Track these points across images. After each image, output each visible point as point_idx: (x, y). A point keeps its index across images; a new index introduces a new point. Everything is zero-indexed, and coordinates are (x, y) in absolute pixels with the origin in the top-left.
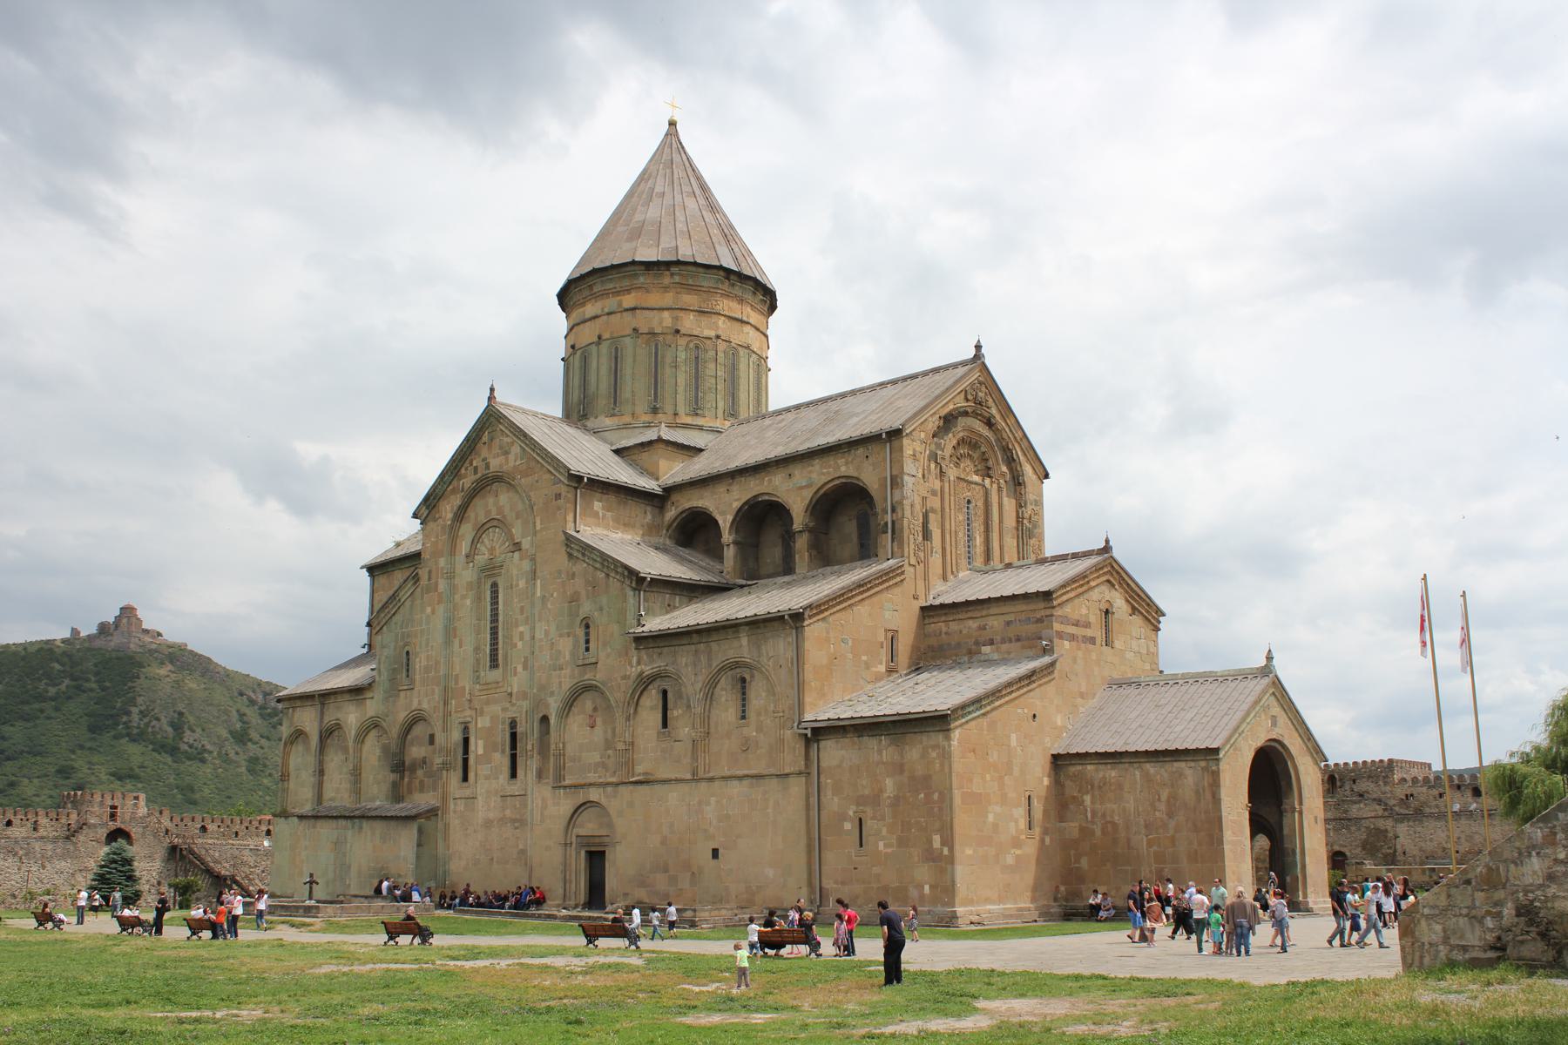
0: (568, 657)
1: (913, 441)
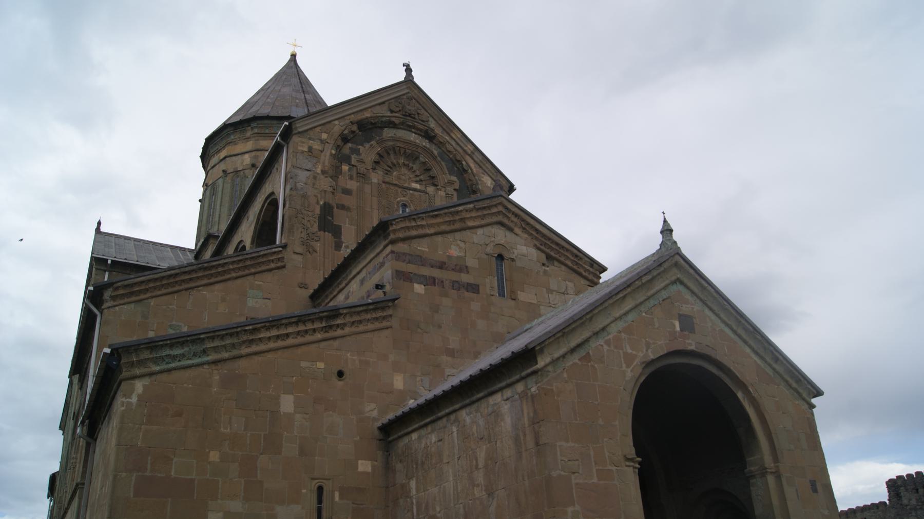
1: (310, 139)
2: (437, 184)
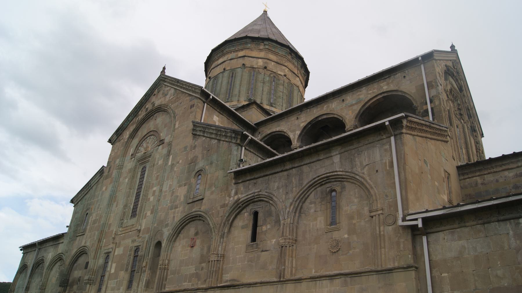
0: (182, 199)
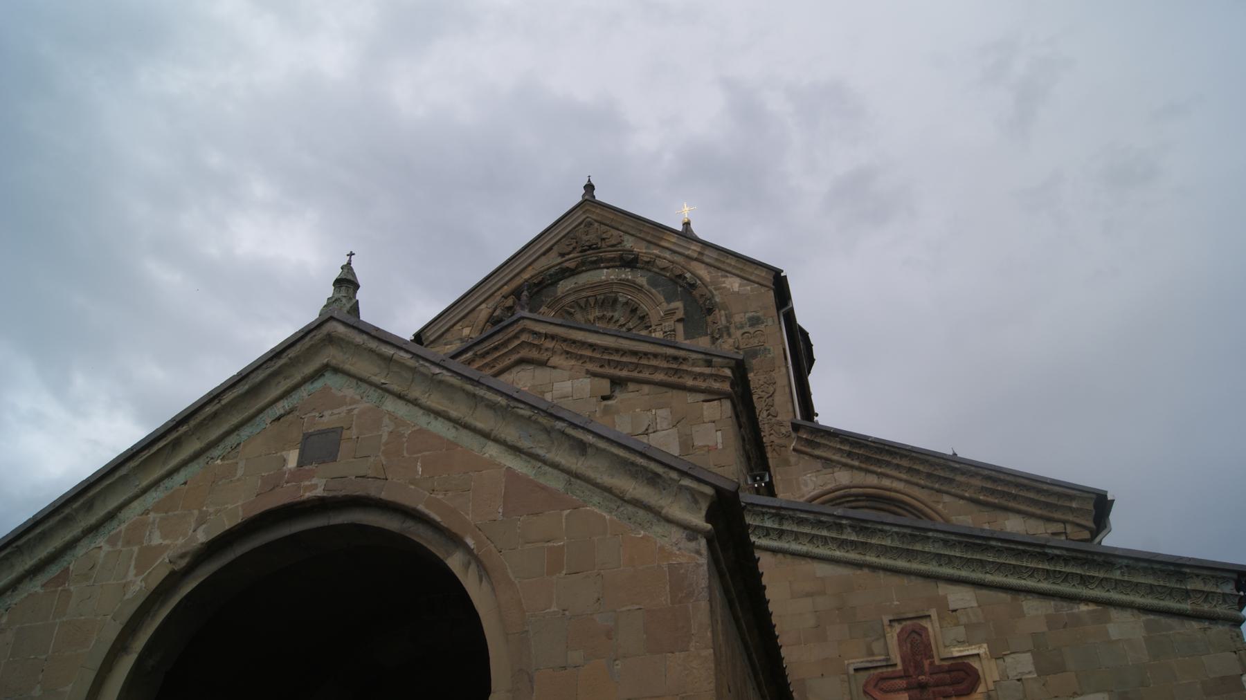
2: (649, 325)
